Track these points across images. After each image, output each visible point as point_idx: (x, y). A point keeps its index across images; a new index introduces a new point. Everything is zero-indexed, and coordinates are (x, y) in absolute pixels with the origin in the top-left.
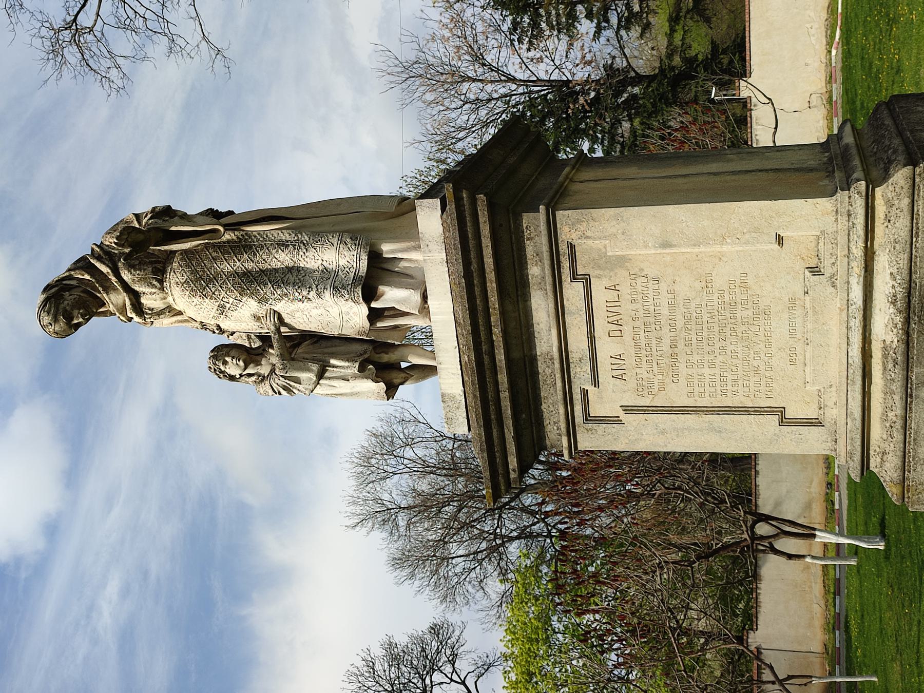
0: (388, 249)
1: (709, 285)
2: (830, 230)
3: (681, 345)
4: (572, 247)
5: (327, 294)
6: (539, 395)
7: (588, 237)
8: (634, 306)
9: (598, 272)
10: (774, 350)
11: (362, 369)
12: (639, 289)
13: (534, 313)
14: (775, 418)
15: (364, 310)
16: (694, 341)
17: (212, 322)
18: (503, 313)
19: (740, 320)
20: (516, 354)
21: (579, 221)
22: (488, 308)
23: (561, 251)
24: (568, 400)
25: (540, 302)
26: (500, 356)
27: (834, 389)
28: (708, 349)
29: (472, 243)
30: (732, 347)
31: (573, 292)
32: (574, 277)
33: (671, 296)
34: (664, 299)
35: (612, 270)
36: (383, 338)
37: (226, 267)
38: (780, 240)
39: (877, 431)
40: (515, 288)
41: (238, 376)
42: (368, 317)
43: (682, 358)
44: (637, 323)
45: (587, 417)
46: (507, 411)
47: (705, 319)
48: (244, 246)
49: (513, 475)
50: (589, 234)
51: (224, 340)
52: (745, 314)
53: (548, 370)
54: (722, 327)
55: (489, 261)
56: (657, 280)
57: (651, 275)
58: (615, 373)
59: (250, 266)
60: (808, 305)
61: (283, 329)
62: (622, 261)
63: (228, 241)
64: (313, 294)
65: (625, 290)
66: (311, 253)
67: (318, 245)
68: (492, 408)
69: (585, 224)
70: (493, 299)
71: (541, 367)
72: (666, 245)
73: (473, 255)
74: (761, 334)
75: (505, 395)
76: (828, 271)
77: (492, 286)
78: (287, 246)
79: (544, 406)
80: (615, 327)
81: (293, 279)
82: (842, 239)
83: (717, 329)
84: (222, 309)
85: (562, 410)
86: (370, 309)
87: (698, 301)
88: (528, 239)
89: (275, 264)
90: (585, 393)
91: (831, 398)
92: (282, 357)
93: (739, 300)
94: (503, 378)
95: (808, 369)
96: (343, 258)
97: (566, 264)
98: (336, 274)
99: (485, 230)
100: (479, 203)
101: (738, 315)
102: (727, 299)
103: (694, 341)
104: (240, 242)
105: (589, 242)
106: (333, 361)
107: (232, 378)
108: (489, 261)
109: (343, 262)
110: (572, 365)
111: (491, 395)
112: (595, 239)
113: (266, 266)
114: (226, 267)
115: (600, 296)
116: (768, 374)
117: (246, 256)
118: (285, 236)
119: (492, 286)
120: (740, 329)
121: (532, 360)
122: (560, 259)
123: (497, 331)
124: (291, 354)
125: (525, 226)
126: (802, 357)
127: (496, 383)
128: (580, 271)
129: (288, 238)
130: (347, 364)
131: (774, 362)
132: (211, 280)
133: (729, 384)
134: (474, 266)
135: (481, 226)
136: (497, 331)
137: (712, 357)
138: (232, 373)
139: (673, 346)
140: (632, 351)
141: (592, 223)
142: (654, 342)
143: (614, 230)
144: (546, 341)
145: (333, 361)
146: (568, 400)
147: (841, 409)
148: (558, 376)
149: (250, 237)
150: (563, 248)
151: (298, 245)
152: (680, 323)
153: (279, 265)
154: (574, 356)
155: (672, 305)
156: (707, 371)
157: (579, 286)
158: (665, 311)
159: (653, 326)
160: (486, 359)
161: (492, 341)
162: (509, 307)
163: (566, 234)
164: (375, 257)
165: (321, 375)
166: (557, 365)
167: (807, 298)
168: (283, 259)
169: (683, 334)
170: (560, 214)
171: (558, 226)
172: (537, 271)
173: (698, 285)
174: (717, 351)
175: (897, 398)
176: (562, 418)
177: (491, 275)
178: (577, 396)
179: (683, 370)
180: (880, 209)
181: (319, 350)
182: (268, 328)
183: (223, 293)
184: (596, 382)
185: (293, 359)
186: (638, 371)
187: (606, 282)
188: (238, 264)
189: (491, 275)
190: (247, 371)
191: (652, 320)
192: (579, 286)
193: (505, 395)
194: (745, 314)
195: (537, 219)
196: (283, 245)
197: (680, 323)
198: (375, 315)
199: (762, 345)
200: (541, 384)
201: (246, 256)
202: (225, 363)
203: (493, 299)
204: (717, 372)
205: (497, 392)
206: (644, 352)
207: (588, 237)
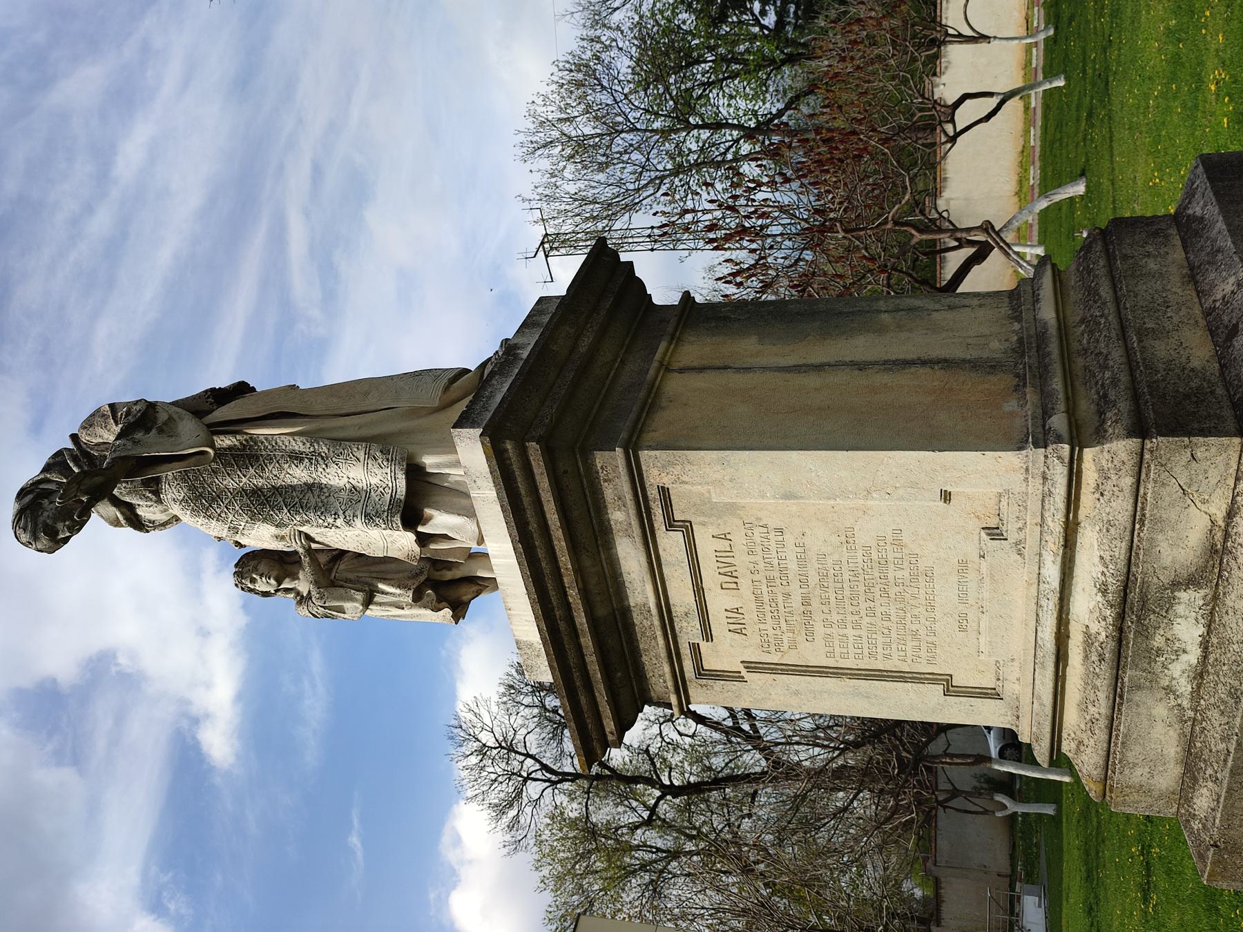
1: (851, 540)
3: (815, 603)
4: (664, 492)
5: (358, 522)
6: (638, 647)
7: (683, 482)
8: (752, 558)
9: (702, 519)
10: (938, 614)
12: (758, 539)
13: (622, 562)
15: (411, 537)
16: (833, 600)
18: (579, 570)
19: (892, 581)
20: (601, 612)
22: (558, 569)
23: (650, 497)
24: (674, 655)
25: (628, 550)
26: (581, 619)
27: (1016, 664)
28: (851, 609)
29: (526, 501)
30: (883, 609)
31: (671, 544)
32: (671, 524)
33: (799, 550)
34: (791, 554)
35: (719, 517)
37: (230, 483)
40: (592, 537)
43: (818, 617)
44: (756, 577)
45: (701, 672)
46: (597, 675)
47: (846, 577)
48: (247, 456)
49: (610, 738)
50: (685, 478)
51: (244, 551)
52: (899, 574)
53: (647, 624)
54: (869, 589)
55: (553, 518)
56: (781, 531)
57: (772, 525)
59: (260, 482)
61: (314, 546)
62: (732, 509)
63: (230, 448)
64: (339, 522)
65: (739, 539)
66: (333, 469)
67: (341, 460)
68: (576, 675)
69: (679, 468)
70: (564, 559)
71: (637, 618)
72: (788, 496)
73: (530, 514)
74: (922, 596)
75: (592, 660)
77: (561, 545)
78: (301, 460)
79: (644, 658)
81: (313, 499)
84: (235, 530)
85: (667, 669)
87: (836, 557)
88: (605, 481)
89: (289, 480)
90: (695, 649)
92: (317, 583)
94: (587, 641)
95: (982, 639)
96: (376, 476)
97: (658, 512)
98: (368, 494)
99: (544, 483)
100: (531, 452)
101: (891, 576)
102: (874, 556)
103: (833, 600)
104: (244, 450)
106: (381, 586)
108: (553, 518)
109: (374, 481)
110: (676, 620)
111: (572, 659)
112: (693, 484)
113: (280, 482)
114: (230, 483)
115: (706, 546)
116: (930, 639)
117: (252, 471)
118: (298, 445)
119: (561, 545)
120: (893, 591)
121: (626, 612)
123: (573, 594)
124: (330, 570)
125: (599, 466)
126: (975, 625)
127: (579, 648)
130: (398, 591)
131: (938, 627)
132: (213, 500)
134: (533, 526)
135: (538, 478)
136: (573, 594)
137: (857, 617)
139: (806, 602)
140: (753, 605)
141: (688, 467)
142: (780, 599)
143: (718, 476)
144: (640, 592)
145: (381, 586)
146: (674, 655)
148: (659, 633)
149: (256, 443)
150: (653, 493)
151: (315, 459)
152: (814, 579)
153: (295, 482)
154: (677, 610)
155: (802, 561)
156: (850, 632)
157: (678, 536)
158: (793, 566)
159: (778, 581)
160: (562, 625)
161: (569, 604)
162: (587, 562)
164: (416, 473)
165: (368, 602)
166: (657, 622)
168: (298, 475)
169: (818, 591)
170: (644, 455)
171: (644, 468)
172: (620, 516)
173: (835, 540)
174: (863, 613)
176: (668, 676)
177: (558, 534)
178: (685, 651)
179: (819, 629)
181: (365, 568)
182: (297, 546)
183: (231, 517)
185: (333, 584)
186: (762, 626)
188: (244, 480)
189: (558, 534)
191: (777, 574)
192: (678, 536)
193: (592, 660)
194: (899, 574)
195: (614, 459)
196: (296, 458)
197: (814, 579)
198: (423, 540)
199: (922, 609)
200: (639, 636)
201: (252, 471)
203: (564, 559)
204: (863, 633)
205: (582, 656)
207: (683, 482)
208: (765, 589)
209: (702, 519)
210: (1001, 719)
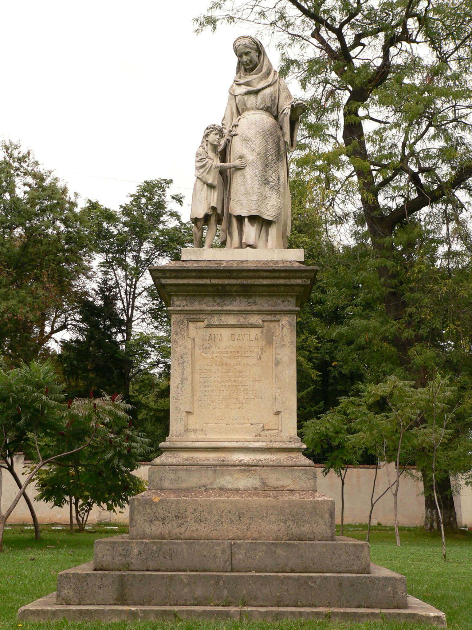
0: (273, 231)
2: (282, 435)
3: (226, 367)
4: (278, 320)
9: (265, 331)
11: (214, 209)
14: (189, 410)
15: (244, 214)
17: (238, 130)
21: (290, 325)
32: (263, 321)
36: (224, 222)
38: (277, 413)
39: (185, 455)
41: (207, 139)
42: (240, 216)
47: (240, 379)
50: (284, 329)
58: (213, 336)
60: (246, 425)
69: (289, 327)
76: (263, 434)
80: (237, 337)
82: (278, 438)
83: (235, 384)
86: (244, 217)
90: (203, 321)
91: (200, 436)
93: (248, 394)
95: (214, 425)
102: (249, 389)
103: (228, 374)
105: (280, 329)
107: (207, 136)
120: (234, 395)
122: (274, 315)
128: (266, 324)
129: (281, 181)
133: (206, 389)
138: (209, 137)
139: (226, 364)
141: (289, 331)
142: (229, 355)
147: (194, 439)
150: (278, 317)
152: (238, 368)
159: (236, 355)
163: (285, 320)
167: (249, 425)
175: (206, 462)
180: (294, 455)
184: (207, 327)
187: (259, 335)
190: (209, 145)
198: (240, 219)
202: (216, 134)
205: (210, 278)
206: (223, 350)
207: (283, 329)
208: (233, 350)
209: (265, 331)
210: (174, 432)
